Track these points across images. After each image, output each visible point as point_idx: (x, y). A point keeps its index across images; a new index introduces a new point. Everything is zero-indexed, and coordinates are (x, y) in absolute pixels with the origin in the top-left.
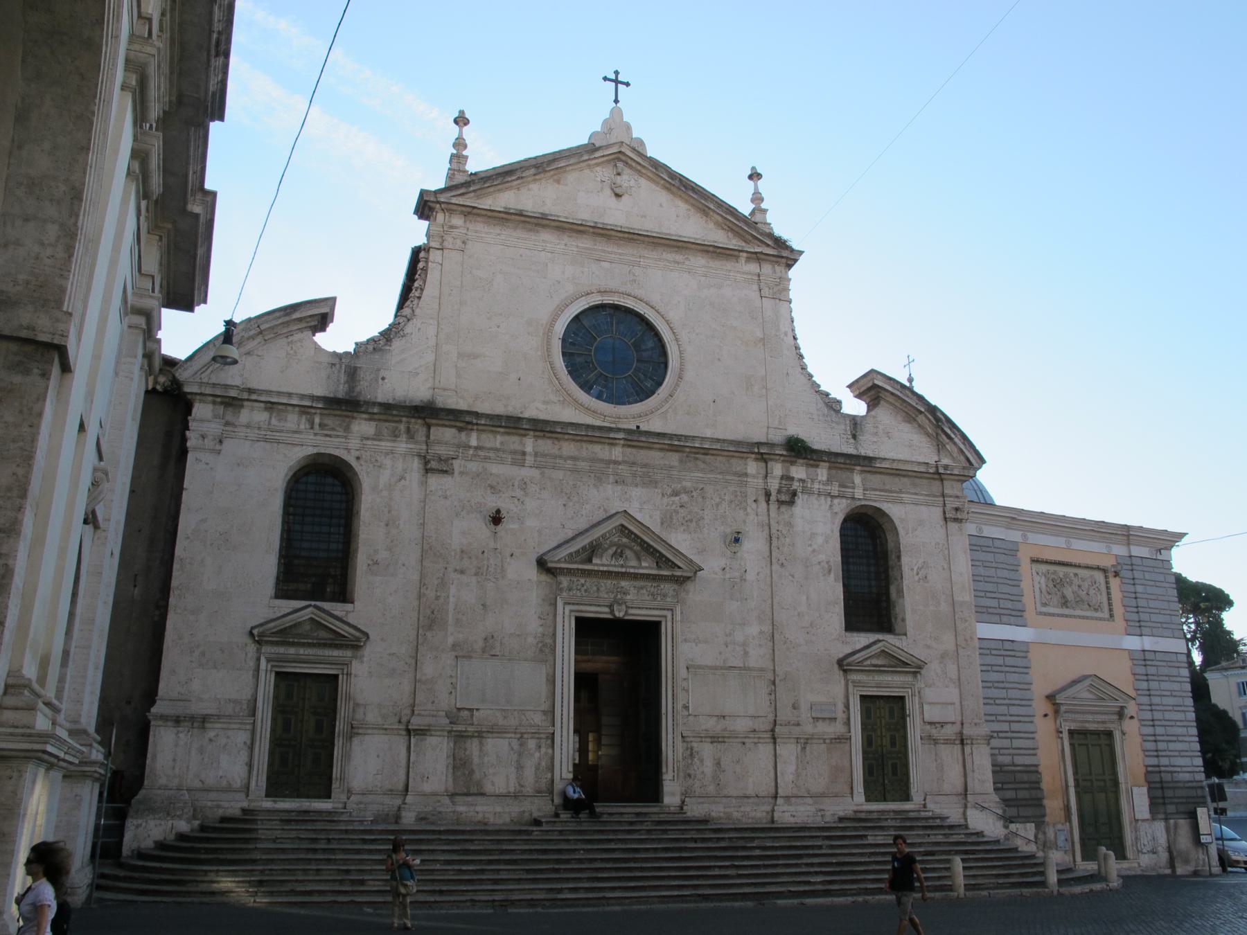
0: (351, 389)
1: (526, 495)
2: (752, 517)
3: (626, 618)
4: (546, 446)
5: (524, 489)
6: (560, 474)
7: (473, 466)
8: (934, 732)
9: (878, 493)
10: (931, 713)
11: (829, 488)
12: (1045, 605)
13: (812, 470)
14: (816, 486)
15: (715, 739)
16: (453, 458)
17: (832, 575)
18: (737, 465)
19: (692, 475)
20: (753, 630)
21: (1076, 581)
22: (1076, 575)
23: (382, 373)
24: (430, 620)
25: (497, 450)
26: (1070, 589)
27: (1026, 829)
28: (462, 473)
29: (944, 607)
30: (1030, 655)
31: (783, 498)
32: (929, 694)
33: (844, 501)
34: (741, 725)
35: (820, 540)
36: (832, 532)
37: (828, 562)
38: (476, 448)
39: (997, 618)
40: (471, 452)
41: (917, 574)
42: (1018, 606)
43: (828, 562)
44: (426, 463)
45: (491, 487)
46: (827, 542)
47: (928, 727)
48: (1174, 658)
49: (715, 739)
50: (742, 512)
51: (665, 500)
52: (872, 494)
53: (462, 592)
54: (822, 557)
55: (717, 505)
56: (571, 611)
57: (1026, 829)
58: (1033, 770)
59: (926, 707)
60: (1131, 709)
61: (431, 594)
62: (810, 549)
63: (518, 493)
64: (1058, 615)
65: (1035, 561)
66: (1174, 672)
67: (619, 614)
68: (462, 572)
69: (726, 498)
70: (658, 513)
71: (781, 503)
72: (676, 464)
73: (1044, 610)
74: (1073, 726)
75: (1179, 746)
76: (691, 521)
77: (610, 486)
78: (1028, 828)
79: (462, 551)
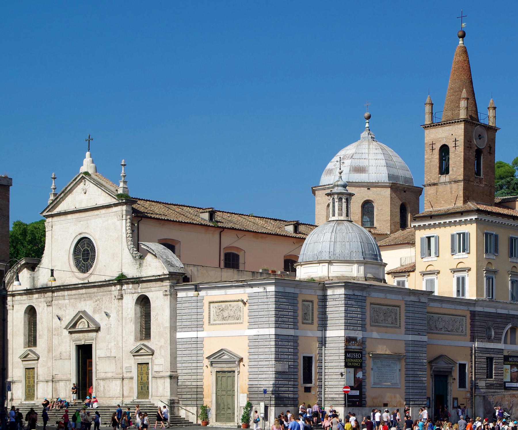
0: (34, 285)
1: (66, 309)
2: (113, 305)
3: (85, 344)
4: (70, 292)
5: (66, 307)
6: (72, 301)
7: (56, 302)
8: (157, 375)
9: (145, 289)
10: (156, 368)
11: (131, 290)
12: (215, 320)
13: (128, 285)
14: (128, 291)
15: (103, 379)
16: (52, 301)
17: (132, 322)
18: (110, 288)
19: (99, 294)
20: (113, 344)
21: (230, 308)
22: (230, 305)
23: (39, 278)
24: (50, 350)
25: (59, 296)
26: (227, 312)
27: (193, 409)
28: (54, 305)
29: (162, 329)
30: (204, 343)
31: (119, 297)
32: (156, 361)
33: (136, 294)
34: (109, 375)
35: (129, 310)
36: (133, 306)
37: (131, 318)
38: (56, 297)
39: (190, 329)
40: (55, 298)
41: (155, 318)
42: (201, 323)
43: (131, 318)
44: (46, 303)
45: (60, 308)
46: (131, 310)
47: (155, 373)
48: (268, 337)
49: (103, 379)
50: (111, 304)
51: (94, 304)
52: (143, 290)
53: (55, 341)
54: (130, 316)
55: (106, 303)
56: (75, 343)
57: (193, 409)
58: (202, 387)
59: (155, 366)
60: (246, 361)
61: (49, 343)
62: (127, 314)
63: (65, 308)
64: (221, 324)
65: (210, 303)
66: (267, 343)
67: (83, 343)
68: (55, 335)
69: (107, 300)
70: (92, 309)
71: (119, 299)
72: (96, 291)
73: (214, 322)
74: (218, 370)
75: (264, 376)
76: (99, 310)
77: (83, 302)
78: (194, 409)
79: (55, 329)
